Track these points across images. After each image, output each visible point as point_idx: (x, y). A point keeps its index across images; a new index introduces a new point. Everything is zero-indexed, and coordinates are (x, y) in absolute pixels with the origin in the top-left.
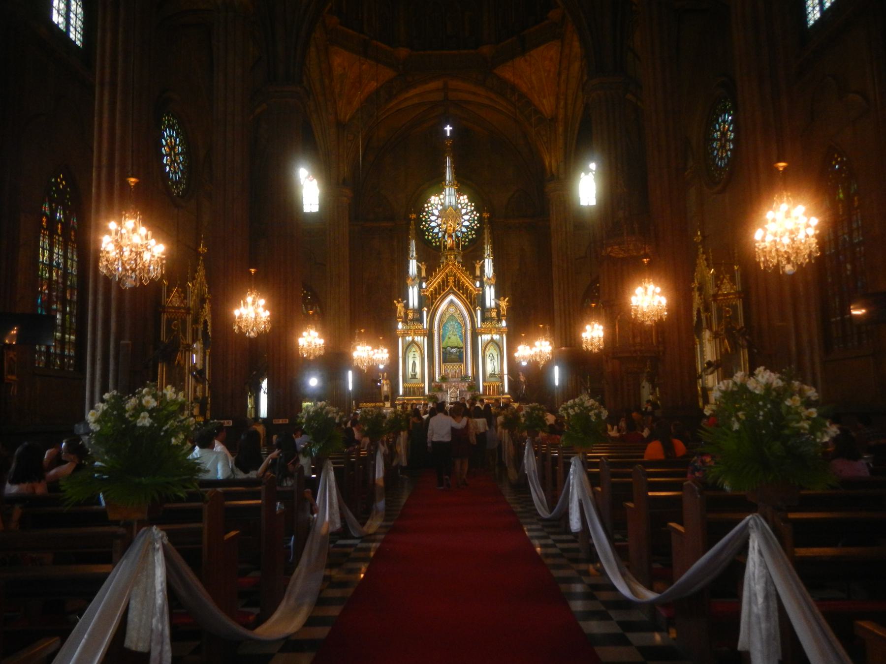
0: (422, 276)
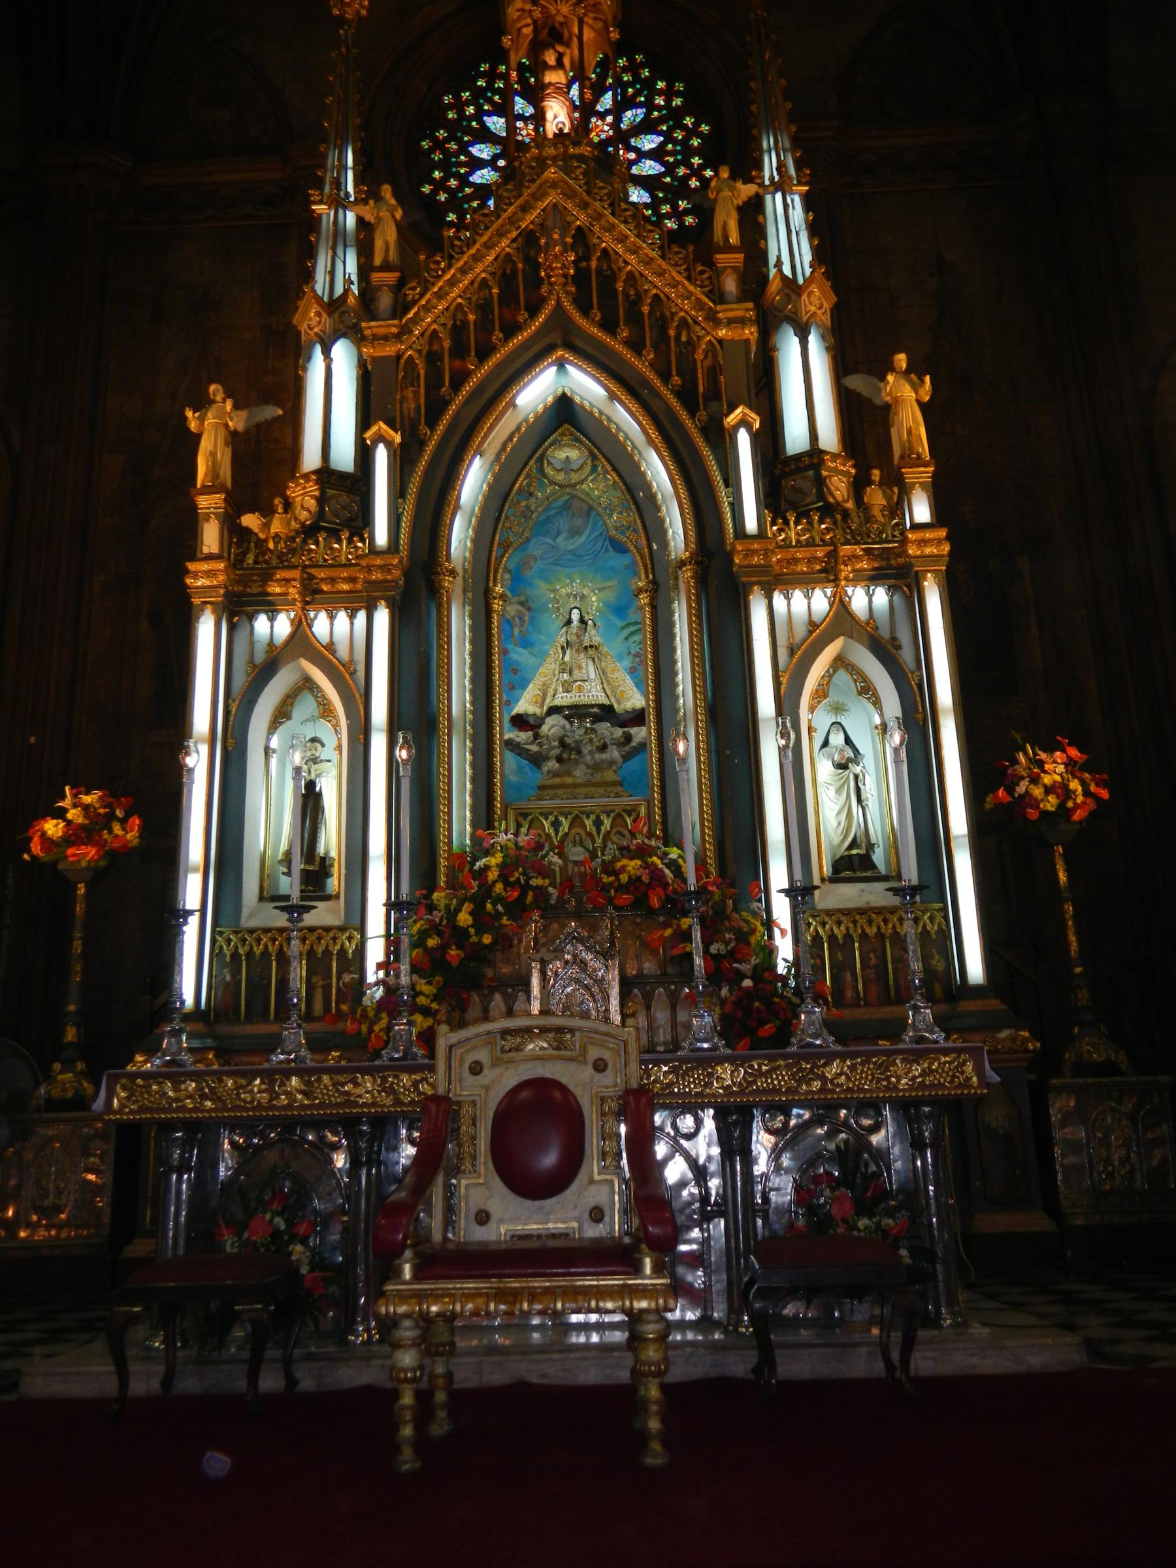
0: (378, 261)
